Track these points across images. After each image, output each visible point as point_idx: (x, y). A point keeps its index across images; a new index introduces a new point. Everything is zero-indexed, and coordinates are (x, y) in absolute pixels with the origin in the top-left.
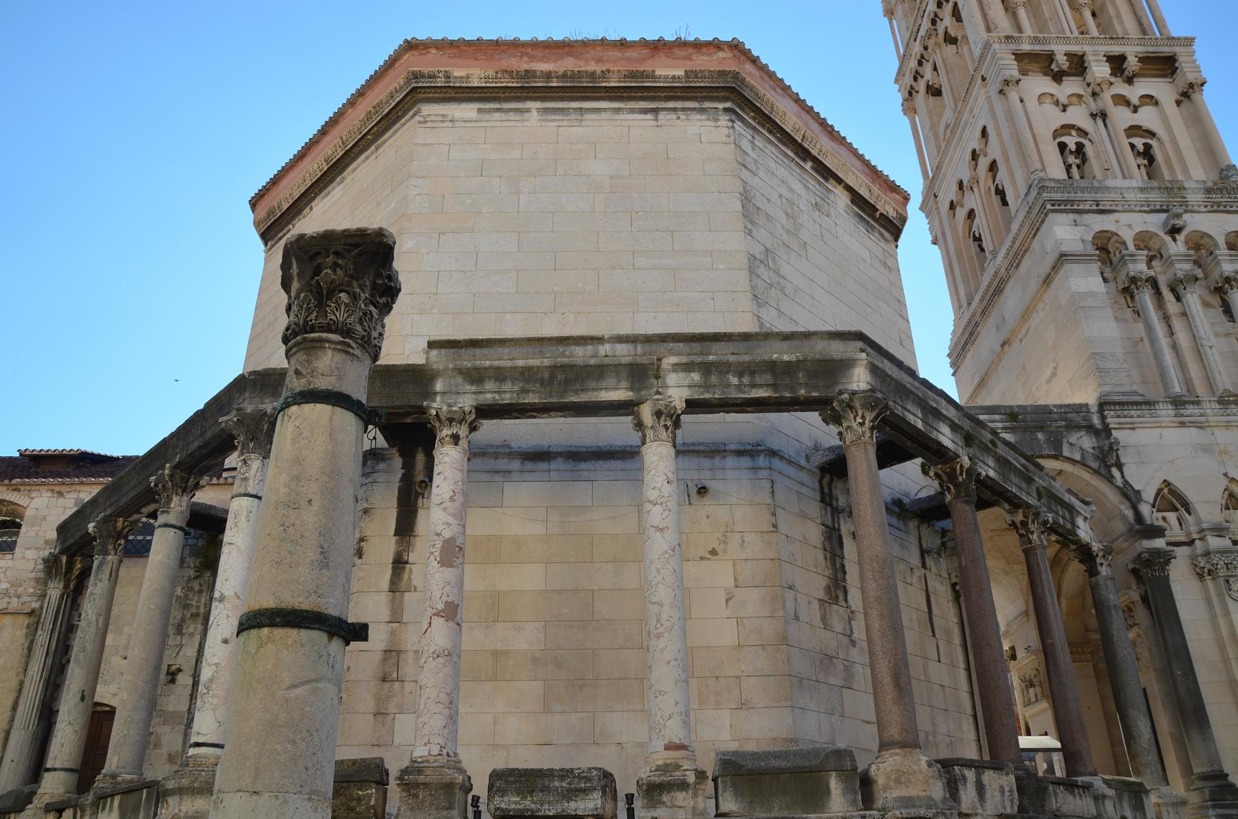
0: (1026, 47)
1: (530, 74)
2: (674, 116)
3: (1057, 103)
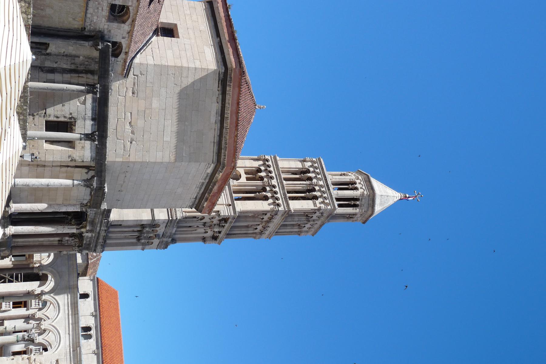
0: (230, 220)
1: (215, 184)
2: (193, 201)
3: (212, 218)
